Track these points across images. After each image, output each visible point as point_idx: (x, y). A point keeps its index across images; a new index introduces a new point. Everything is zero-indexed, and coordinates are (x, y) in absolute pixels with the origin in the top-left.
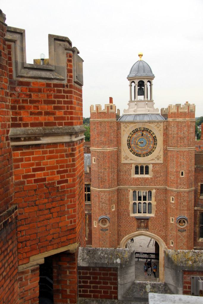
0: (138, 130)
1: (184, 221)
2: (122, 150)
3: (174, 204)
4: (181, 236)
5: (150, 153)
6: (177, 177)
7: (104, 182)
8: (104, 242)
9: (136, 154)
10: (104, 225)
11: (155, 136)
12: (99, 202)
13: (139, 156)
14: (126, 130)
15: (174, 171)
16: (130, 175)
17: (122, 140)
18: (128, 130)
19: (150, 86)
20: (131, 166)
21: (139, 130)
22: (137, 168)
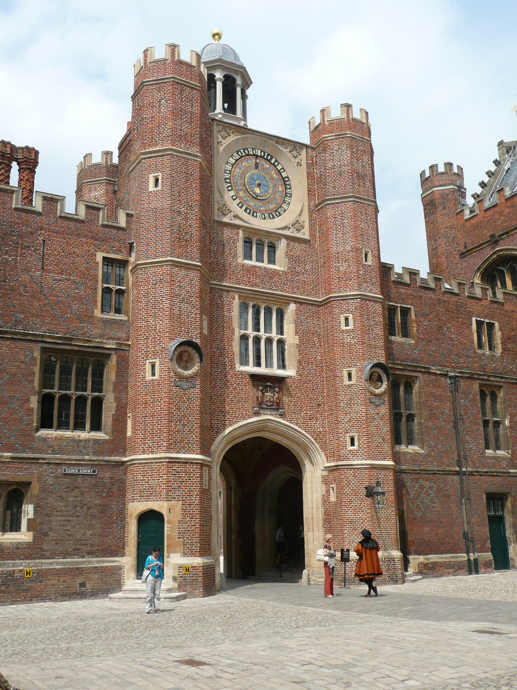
0: (249, 152)
1: (380, 376)
2: (216, 188)
3: (352, 331)
4: (376, 416)
5: (277, 214)
6: (358, 262)
7: (186, 241)
8: (184, 425)
9: (244, 207)
10: (186, 368)
11: (287, 177)
12: (173, 296)
13: (253, 215)
14: (223, 141)
15: (348, 248)
16: (235, 256)
17: (215, 162)
18: (229, 143)
19: (242, 98)
20: (238, 233)
21: (252, 153)
22: (248, 242)
